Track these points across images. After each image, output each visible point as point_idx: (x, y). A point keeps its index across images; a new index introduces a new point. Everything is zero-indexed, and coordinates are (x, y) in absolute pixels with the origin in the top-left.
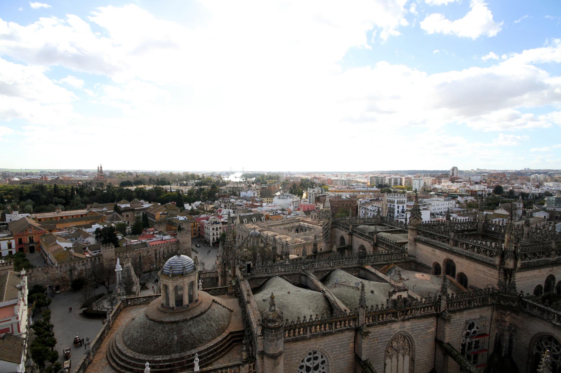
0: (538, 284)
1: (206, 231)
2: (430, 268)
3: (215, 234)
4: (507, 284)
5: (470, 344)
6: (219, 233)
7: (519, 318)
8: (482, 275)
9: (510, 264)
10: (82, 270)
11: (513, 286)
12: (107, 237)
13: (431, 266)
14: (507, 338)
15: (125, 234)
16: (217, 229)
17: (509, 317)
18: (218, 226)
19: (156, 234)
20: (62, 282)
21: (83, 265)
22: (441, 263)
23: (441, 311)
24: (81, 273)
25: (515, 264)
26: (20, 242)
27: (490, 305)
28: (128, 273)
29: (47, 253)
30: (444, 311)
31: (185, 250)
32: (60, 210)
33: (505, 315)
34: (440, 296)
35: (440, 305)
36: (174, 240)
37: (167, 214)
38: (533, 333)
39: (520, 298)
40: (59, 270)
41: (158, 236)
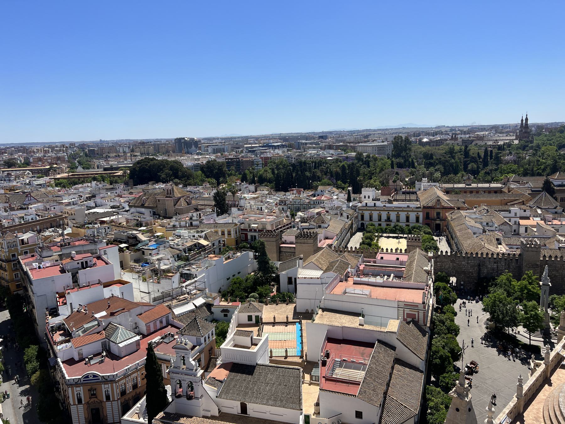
10: (493, 269)
21: (495, 263)
26: (427, 217)
29: (454, 236)
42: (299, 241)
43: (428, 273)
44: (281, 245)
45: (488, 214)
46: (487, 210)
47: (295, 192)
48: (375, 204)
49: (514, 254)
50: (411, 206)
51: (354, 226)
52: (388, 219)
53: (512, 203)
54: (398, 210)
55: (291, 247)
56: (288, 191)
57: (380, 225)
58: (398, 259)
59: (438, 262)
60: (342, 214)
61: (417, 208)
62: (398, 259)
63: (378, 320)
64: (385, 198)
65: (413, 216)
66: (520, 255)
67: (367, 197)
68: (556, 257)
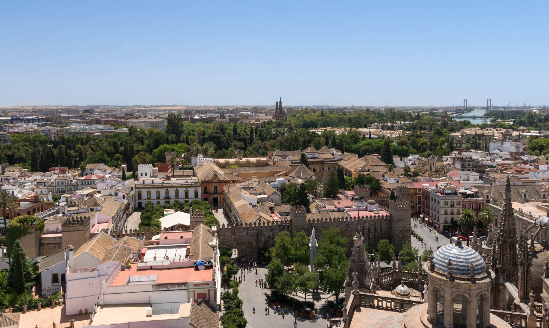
1: (432, 204)
3: (449, 211)
6: (455, 210)
10: (269, 237)
12: (297, 197)
15: (316, 196)
16: (452, 206)
18: (455, 199)
19: (356, 199)
20: (248, 248)
21: (271, 230)
24: (268, 241)
26: (206, 192)
28: (359, 256)
29: (232, 208)
31: (401, 232)
32: (241, 156)
36: (384, 213)
37: (369, 171)
40: (246, 232)
41: (359, 204)
42: (67, 229)
43: (213, 247)
44: (44, 236)
45: (260, 186)
46: (259, 182)
47: (57, 171)
48: (153, 181)
49: (286, 221)
50: (189, 181)
51: (131, 206)
52: (167, 197)
53: (278, 174)
54: (177, 187)
55: (55, 237)
56: (48, 171)
57: (158, 203)
58: (182, 237)
59: (220, 235)
60: (116, 194)
61: (196, 183)
62: (182, 237)
63: (168, 306)
64: (163, 174)
65: (191, 192)
66: (291, 221)
67: (144, 174)
68: (318, 219)
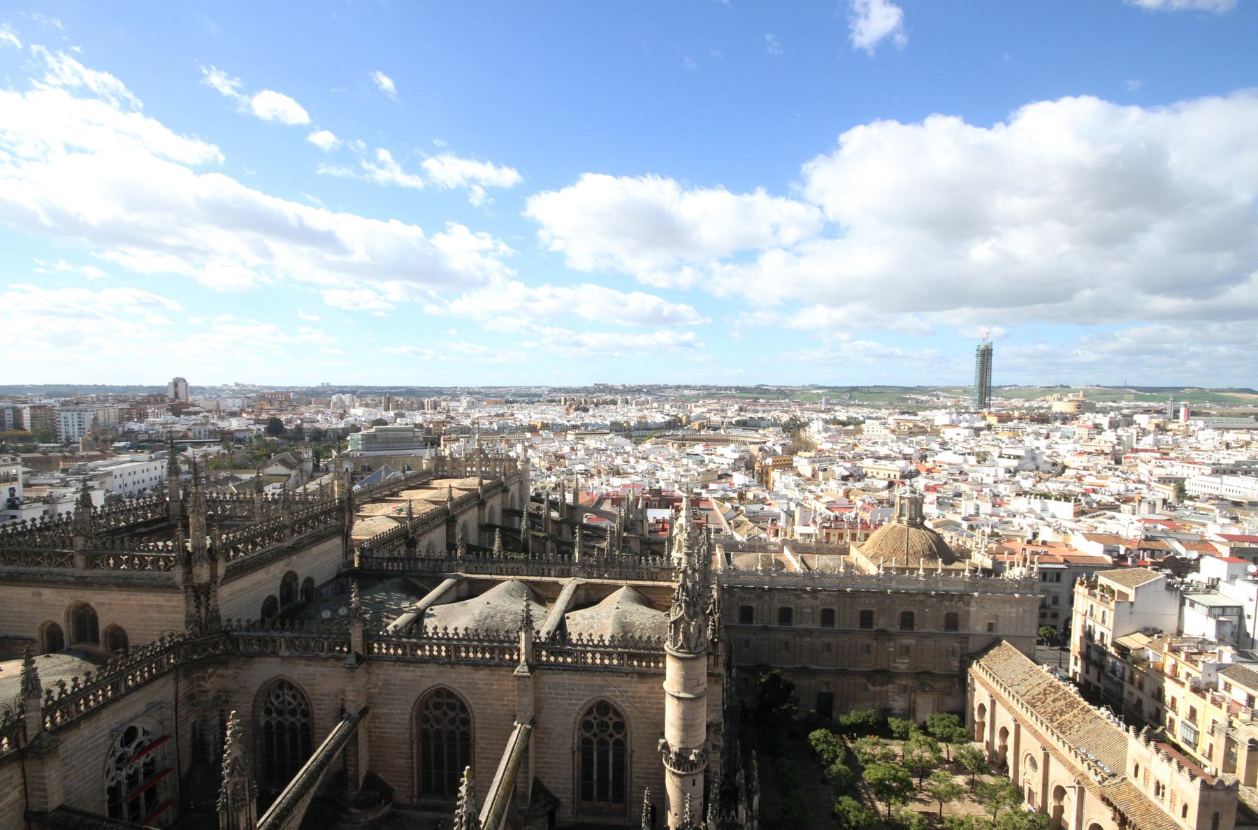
0: (266, 596)
2: (33, 641)
4: (203, 616)
5: (132, 778)
7: (231, 672)
8: (156, 615)
9: (202, 573)
11: (215, 616)
13: (36, 634)
14: (216, 721)
17: (213, 679)
22: (61, 621)
23: (30, 739)
25: (213, 571)
27: (169, 671)
30: (38, 737)
33: (203, 678)
34: (21, 706)
35: (25, 727)
38: (254, 690)
39: (227, 633)
